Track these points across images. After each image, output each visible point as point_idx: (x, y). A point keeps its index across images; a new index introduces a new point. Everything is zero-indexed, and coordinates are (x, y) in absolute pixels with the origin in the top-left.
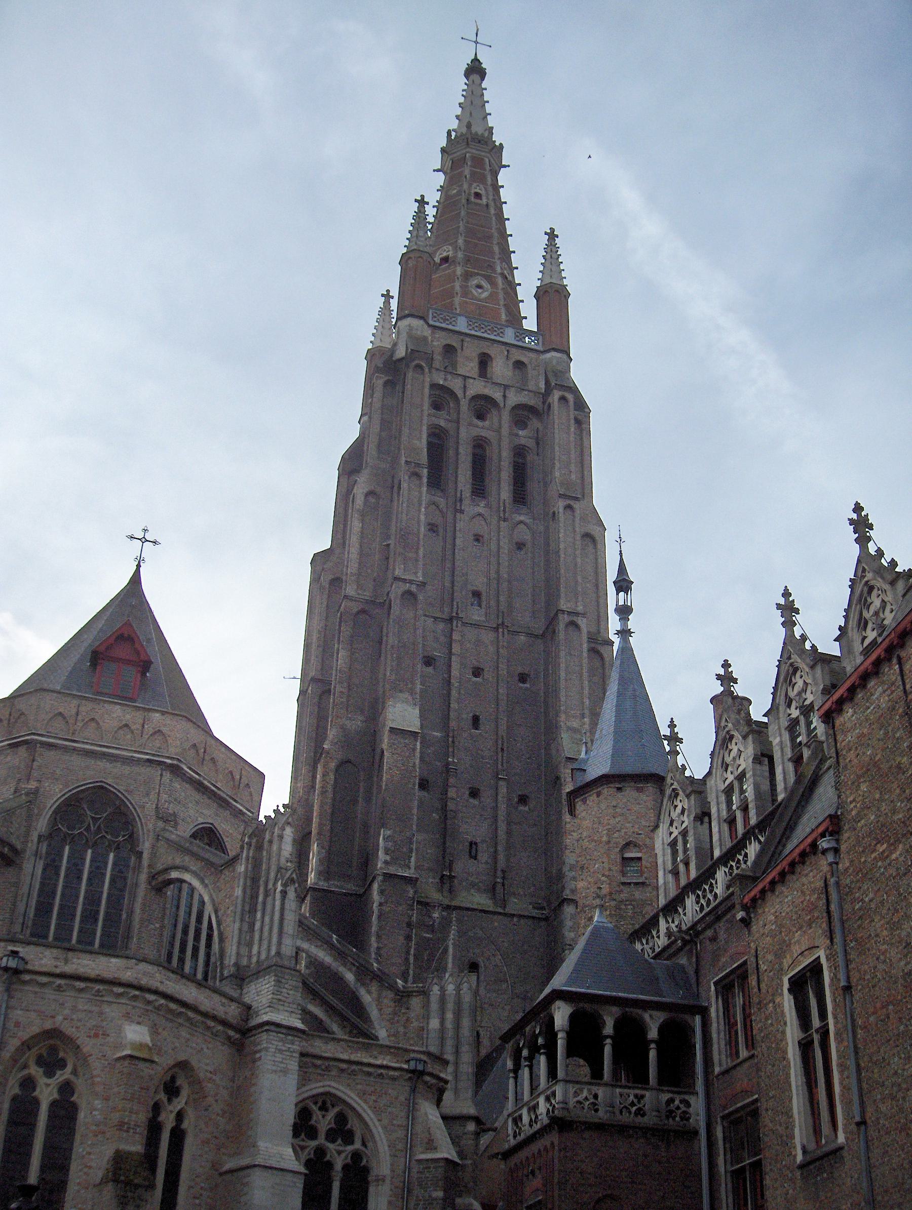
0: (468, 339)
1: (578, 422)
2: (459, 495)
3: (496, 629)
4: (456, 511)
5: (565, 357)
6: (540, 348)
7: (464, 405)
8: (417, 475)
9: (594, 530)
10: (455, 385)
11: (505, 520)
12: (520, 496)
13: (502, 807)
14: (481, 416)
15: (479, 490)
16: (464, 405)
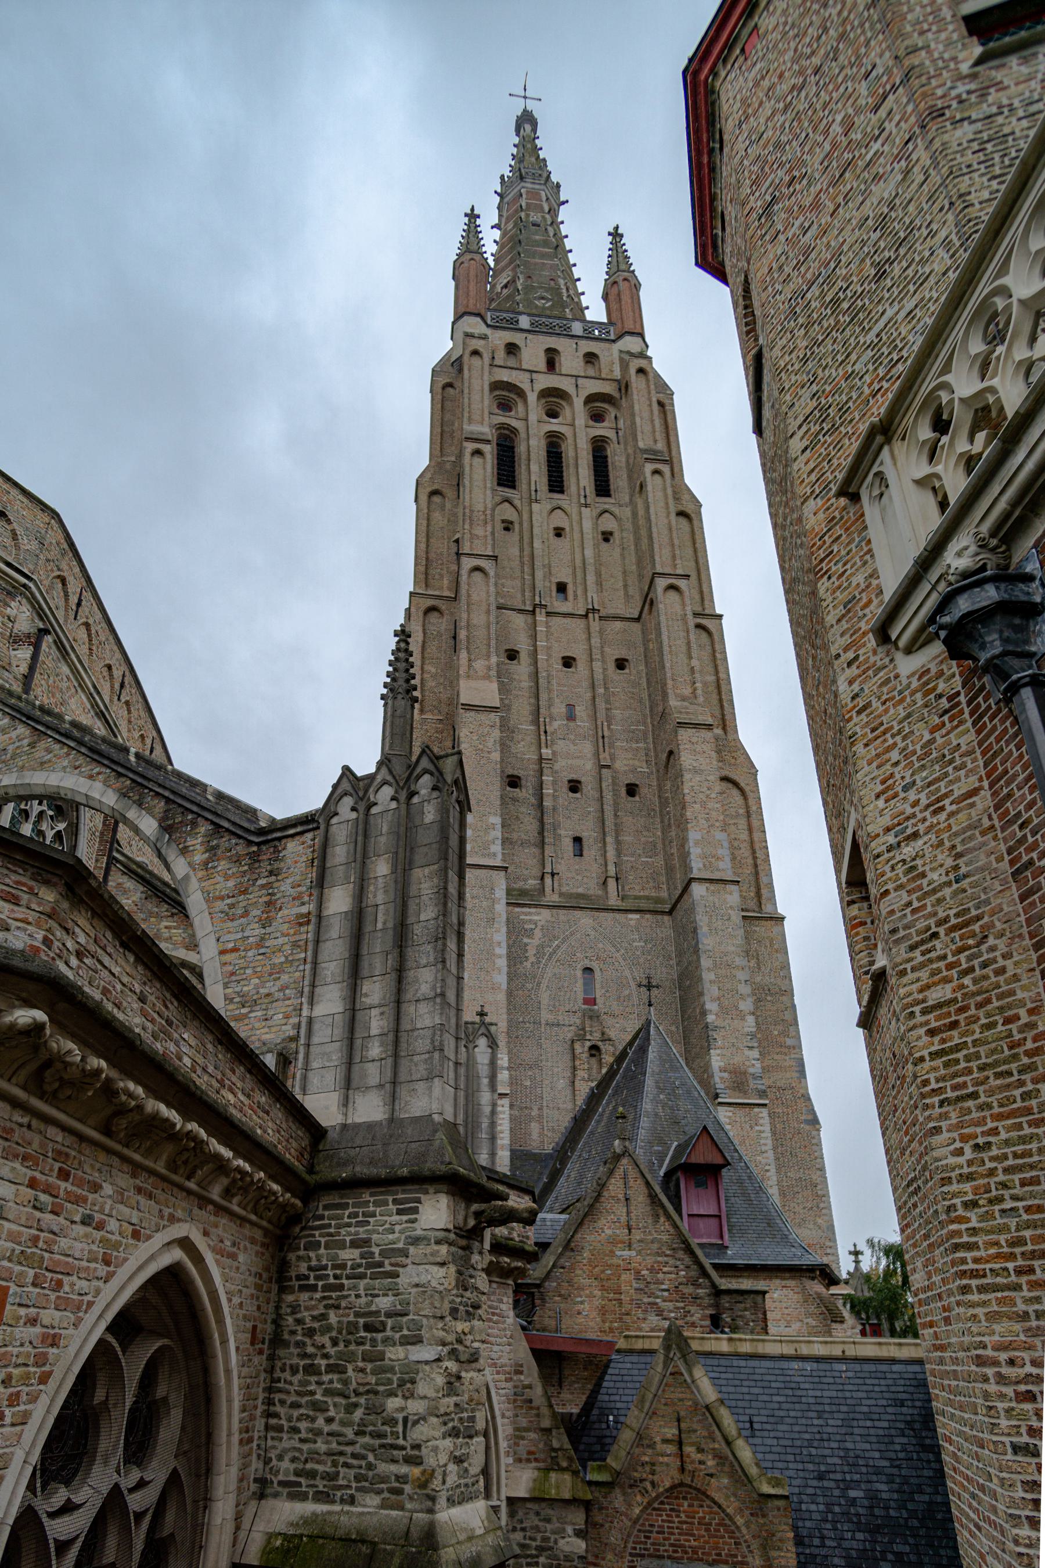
0: (530, 336)
1: (661, 404)
2: (533, 488)
3: (586, 616)
4: (531, 501)
5: (640, 339)
6: (612, 337)
7: (532, 397)
8: (478, 452)
9: (689, 508)
10: (520, 379)
11: (586, 506)
12: (603, 488)
13: (608, 797)
14: (552, 414)
15: (556, 483)
16: (532, 397)
